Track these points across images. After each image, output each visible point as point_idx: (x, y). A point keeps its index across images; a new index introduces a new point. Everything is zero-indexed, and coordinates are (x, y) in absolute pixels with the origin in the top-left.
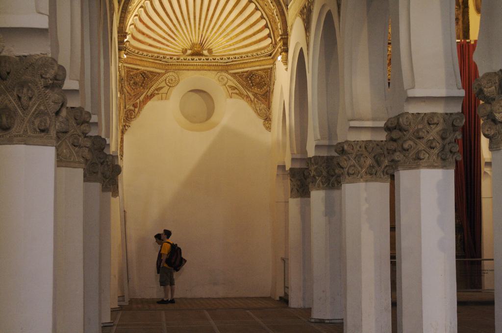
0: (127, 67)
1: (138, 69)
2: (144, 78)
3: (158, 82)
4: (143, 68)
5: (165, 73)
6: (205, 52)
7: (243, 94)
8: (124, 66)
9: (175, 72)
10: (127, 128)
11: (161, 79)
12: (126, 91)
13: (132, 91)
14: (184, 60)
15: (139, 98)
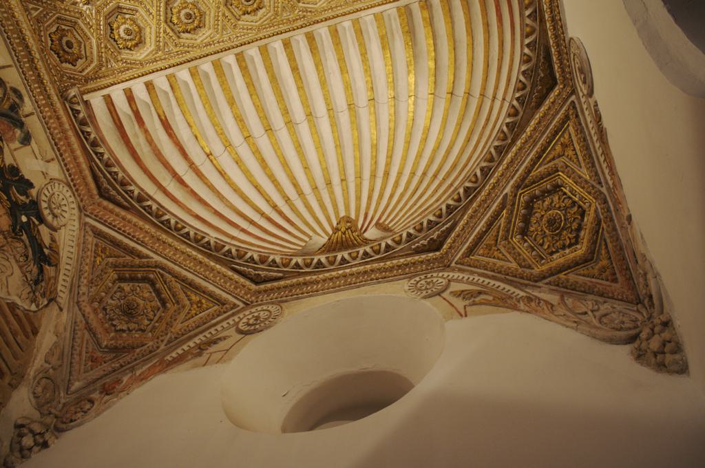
0: (94, 229)
1: (132, 252)
2: (163, 302)
3: (212, 330)
4: (157, 258)
5: (243, 309)
6: (372, 233)
7: (510, 298)
8: (86, 224)
9: (272, 303)
10: (28, 441)
11: (225, 324)
12: (80, 317)
13: (107, 331)
14: (308, 265)
15: (132, 369)
